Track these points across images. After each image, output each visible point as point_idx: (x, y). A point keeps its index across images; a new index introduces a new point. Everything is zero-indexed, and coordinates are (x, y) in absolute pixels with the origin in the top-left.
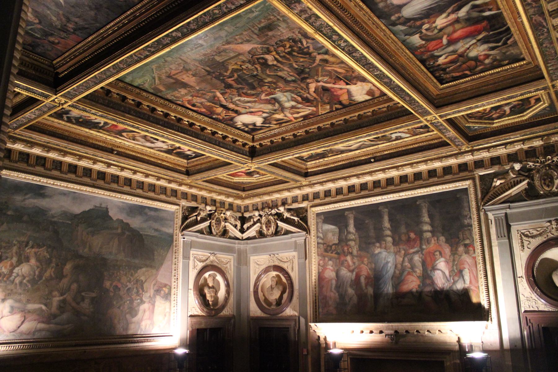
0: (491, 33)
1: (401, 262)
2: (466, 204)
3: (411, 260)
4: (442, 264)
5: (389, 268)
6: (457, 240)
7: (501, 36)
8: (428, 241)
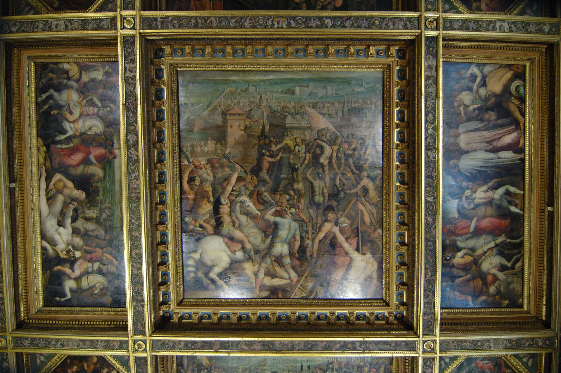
0: (508, 240)
7: (514, 252)
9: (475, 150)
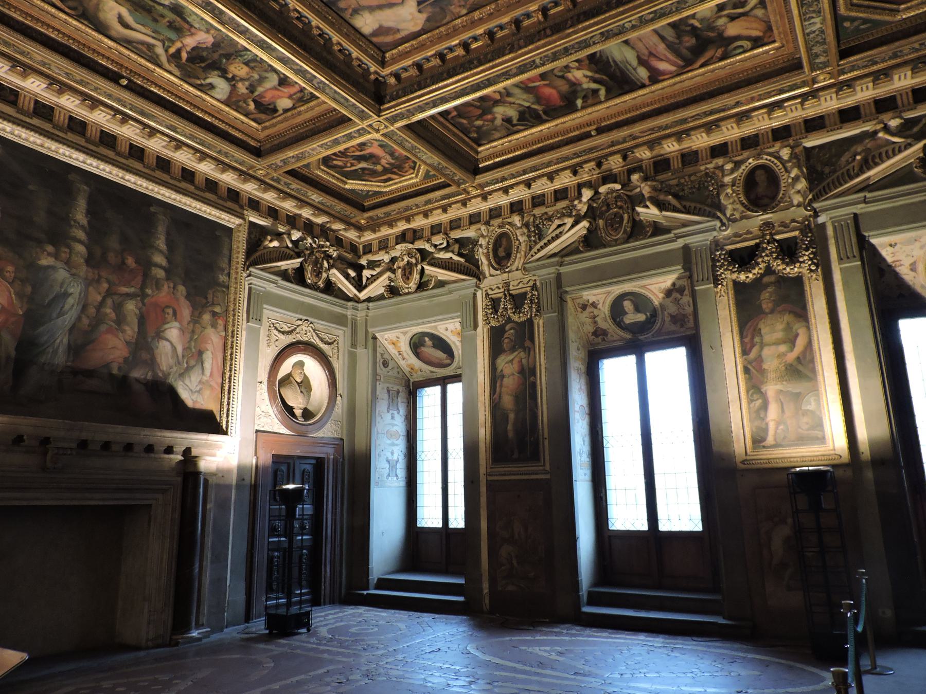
1: (96, 304)
2: (226, 251)
3: (118, 308)
4: (173, 332)
5: (67, 307)
6: (204, 301)
8: (158, 285)
9: (633, 48)
